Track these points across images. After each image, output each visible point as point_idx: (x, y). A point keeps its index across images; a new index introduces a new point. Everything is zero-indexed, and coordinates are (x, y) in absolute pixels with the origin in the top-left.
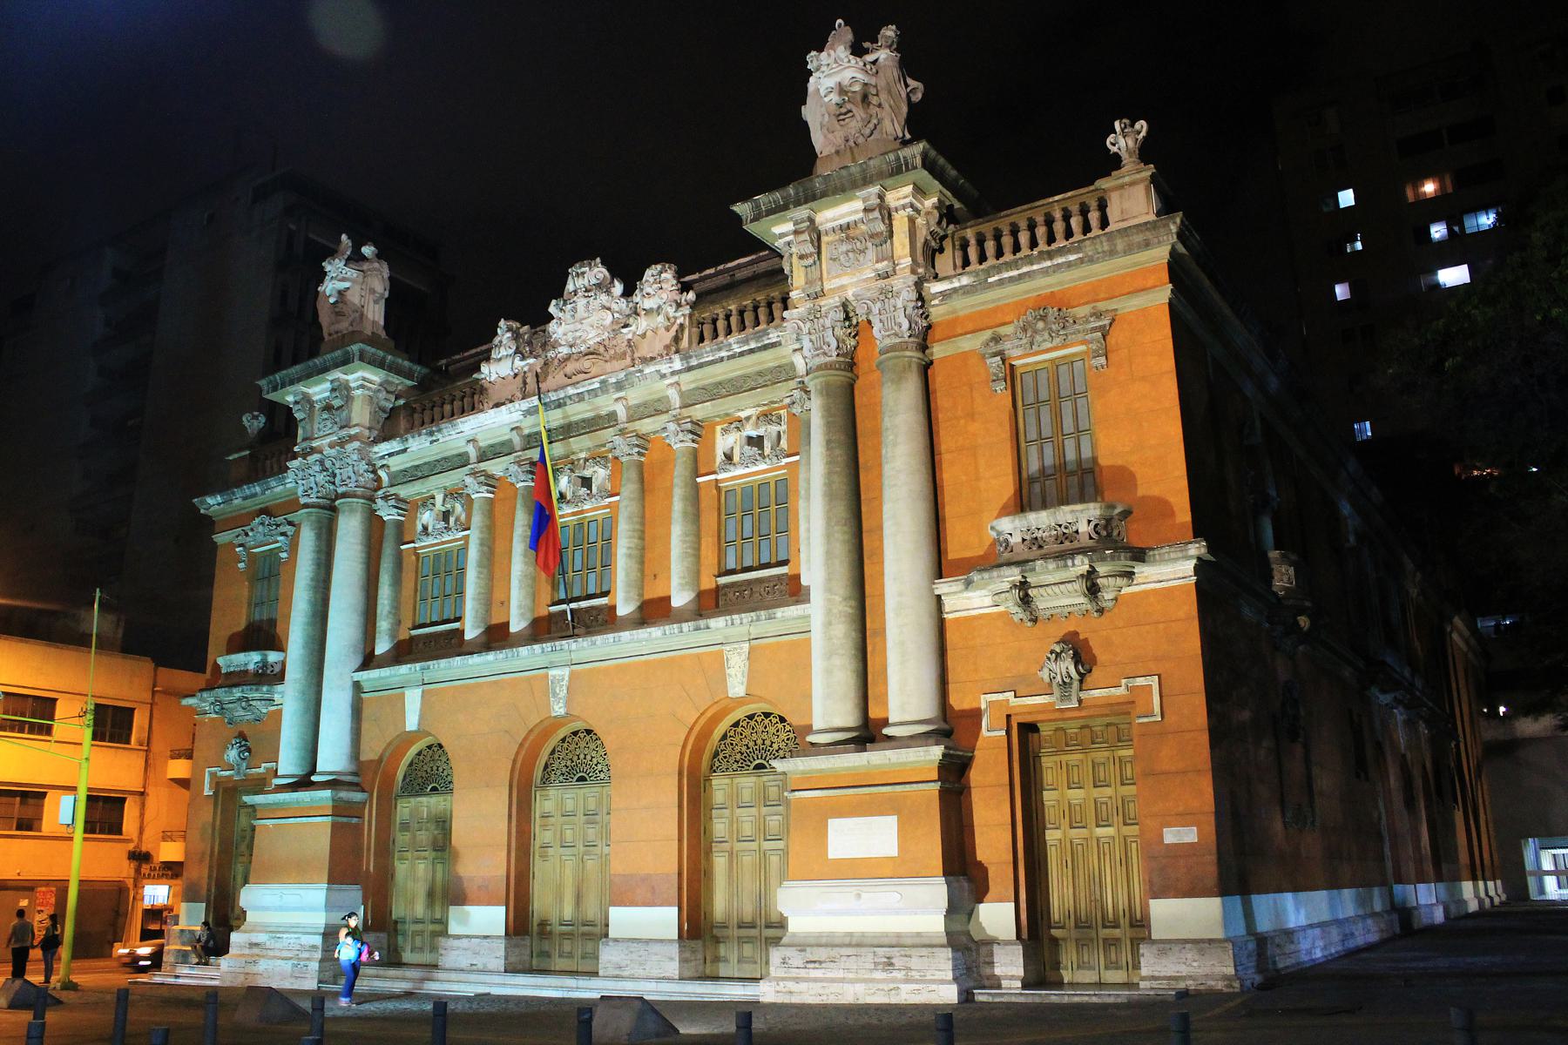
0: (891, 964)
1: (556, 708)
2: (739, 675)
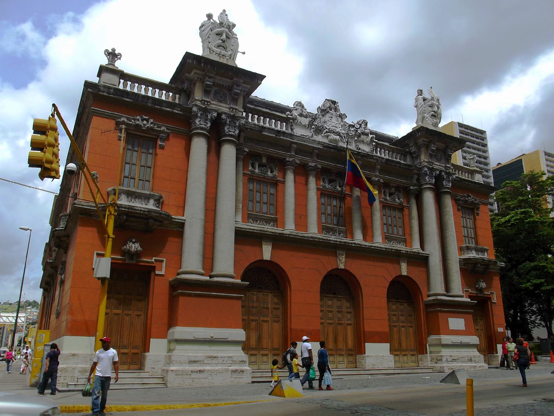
0: (471, 360)
1: (341, 265)
2: (405, 269)
